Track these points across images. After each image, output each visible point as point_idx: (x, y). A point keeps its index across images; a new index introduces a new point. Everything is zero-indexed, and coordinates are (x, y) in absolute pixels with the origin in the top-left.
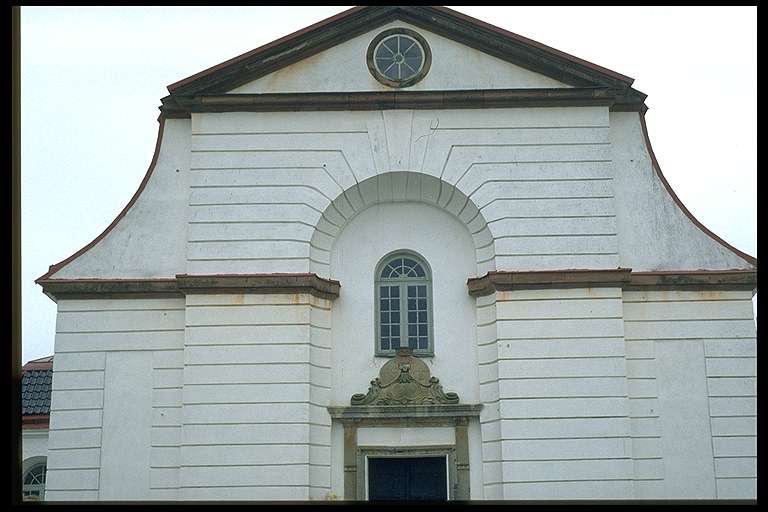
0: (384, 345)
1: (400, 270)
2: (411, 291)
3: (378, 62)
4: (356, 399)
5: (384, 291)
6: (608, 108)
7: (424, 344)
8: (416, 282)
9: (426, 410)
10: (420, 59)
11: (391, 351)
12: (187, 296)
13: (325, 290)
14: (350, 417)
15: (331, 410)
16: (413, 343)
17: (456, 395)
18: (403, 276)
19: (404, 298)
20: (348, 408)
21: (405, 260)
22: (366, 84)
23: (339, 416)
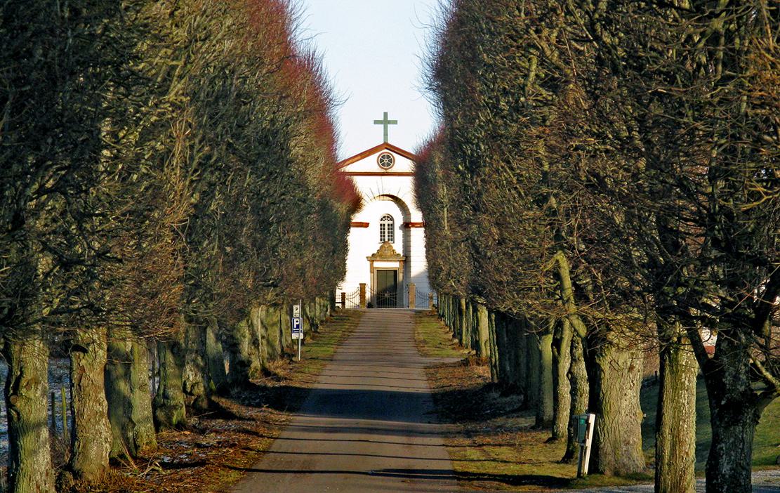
0: (381, 240)
2: (388, 225)
3: (381, 161)
5: (381, 225)
10: (391, 161)
13: (366, 225)
14: (373, 258)
16: (389, 240)
18: (386, 221)
19: (386, 227)
22: (377, 169)
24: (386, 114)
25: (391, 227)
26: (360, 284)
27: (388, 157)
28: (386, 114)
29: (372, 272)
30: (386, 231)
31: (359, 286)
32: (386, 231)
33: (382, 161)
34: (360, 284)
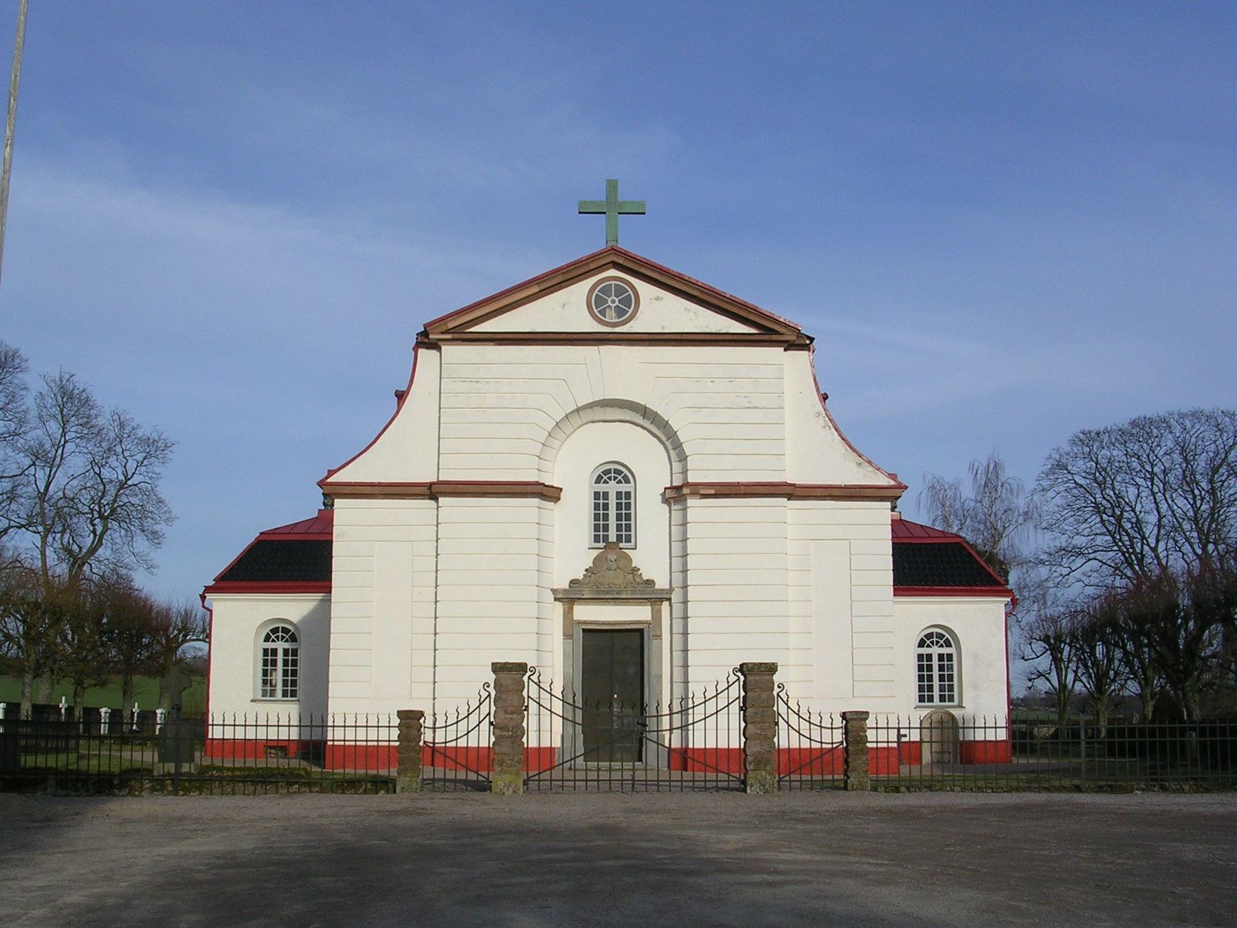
0: (597, 539)
1: (610, 478)
2: (619, 494)
3: (596, 304)
4: (573, 582)
5: (597, 495)
6: (783, 349)
7: (628, 540)
8: (624, 488)
9: (629, 592)
10: (628, 304)
11: (602, 545)
12: (440, 499)
13: (549, 493)
14: (569, 597)
15: (553, 590)
16: (619, 538)
17: (653, 581)
18: (612, 483)
20: (565, 590)
21: (614, 469)
22: (588, 325)
23: (560, 596)
24: (612, 186)
25: (626, 503)
26: (498, 668)
27: (619, 291)
28: (612, 186)
29: (567, 635)
30: (612, 512)
31: (491, 678)
32: (612, 512)
33: (600, 301)
34: (498, 668)
